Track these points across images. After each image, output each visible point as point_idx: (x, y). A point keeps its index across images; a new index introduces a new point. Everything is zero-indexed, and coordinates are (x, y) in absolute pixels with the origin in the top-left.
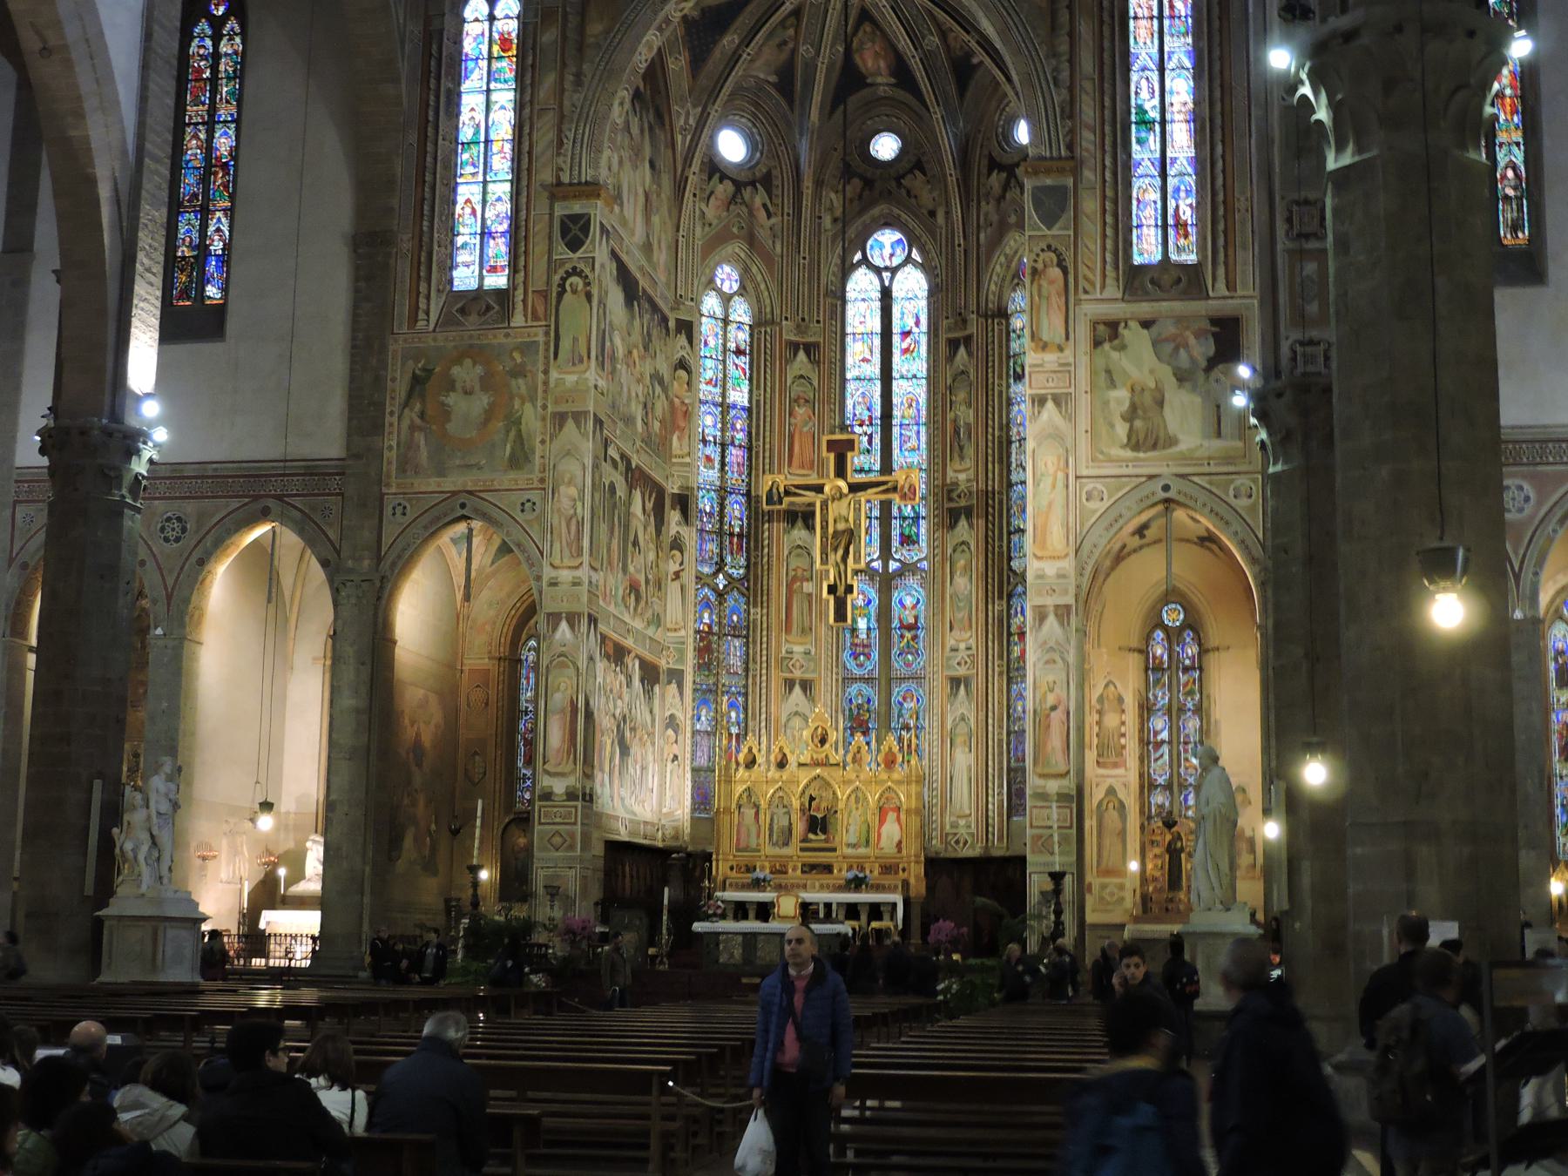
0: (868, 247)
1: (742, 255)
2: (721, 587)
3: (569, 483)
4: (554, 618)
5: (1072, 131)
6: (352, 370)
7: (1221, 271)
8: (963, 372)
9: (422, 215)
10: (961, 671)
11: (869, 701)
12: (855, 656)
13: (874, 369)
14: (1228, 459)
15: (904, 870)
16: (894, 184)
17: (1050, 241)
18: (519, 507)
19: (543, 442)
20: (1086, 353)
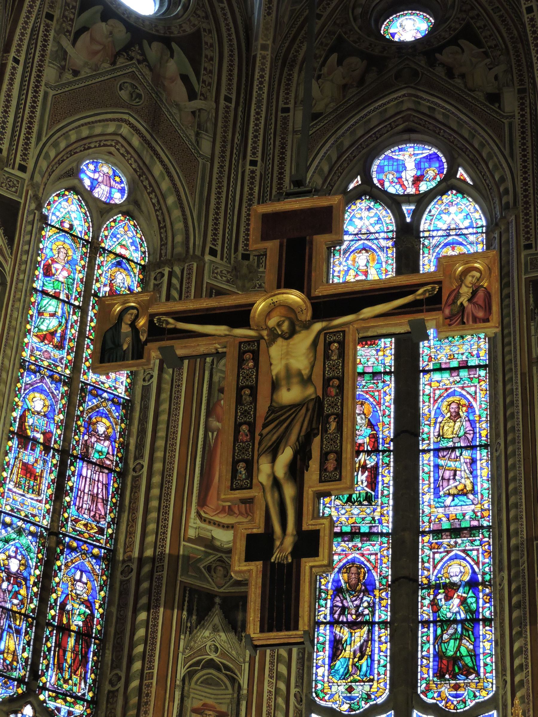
0: (374, 168)
1: (136, 141)
16: (423, 61)
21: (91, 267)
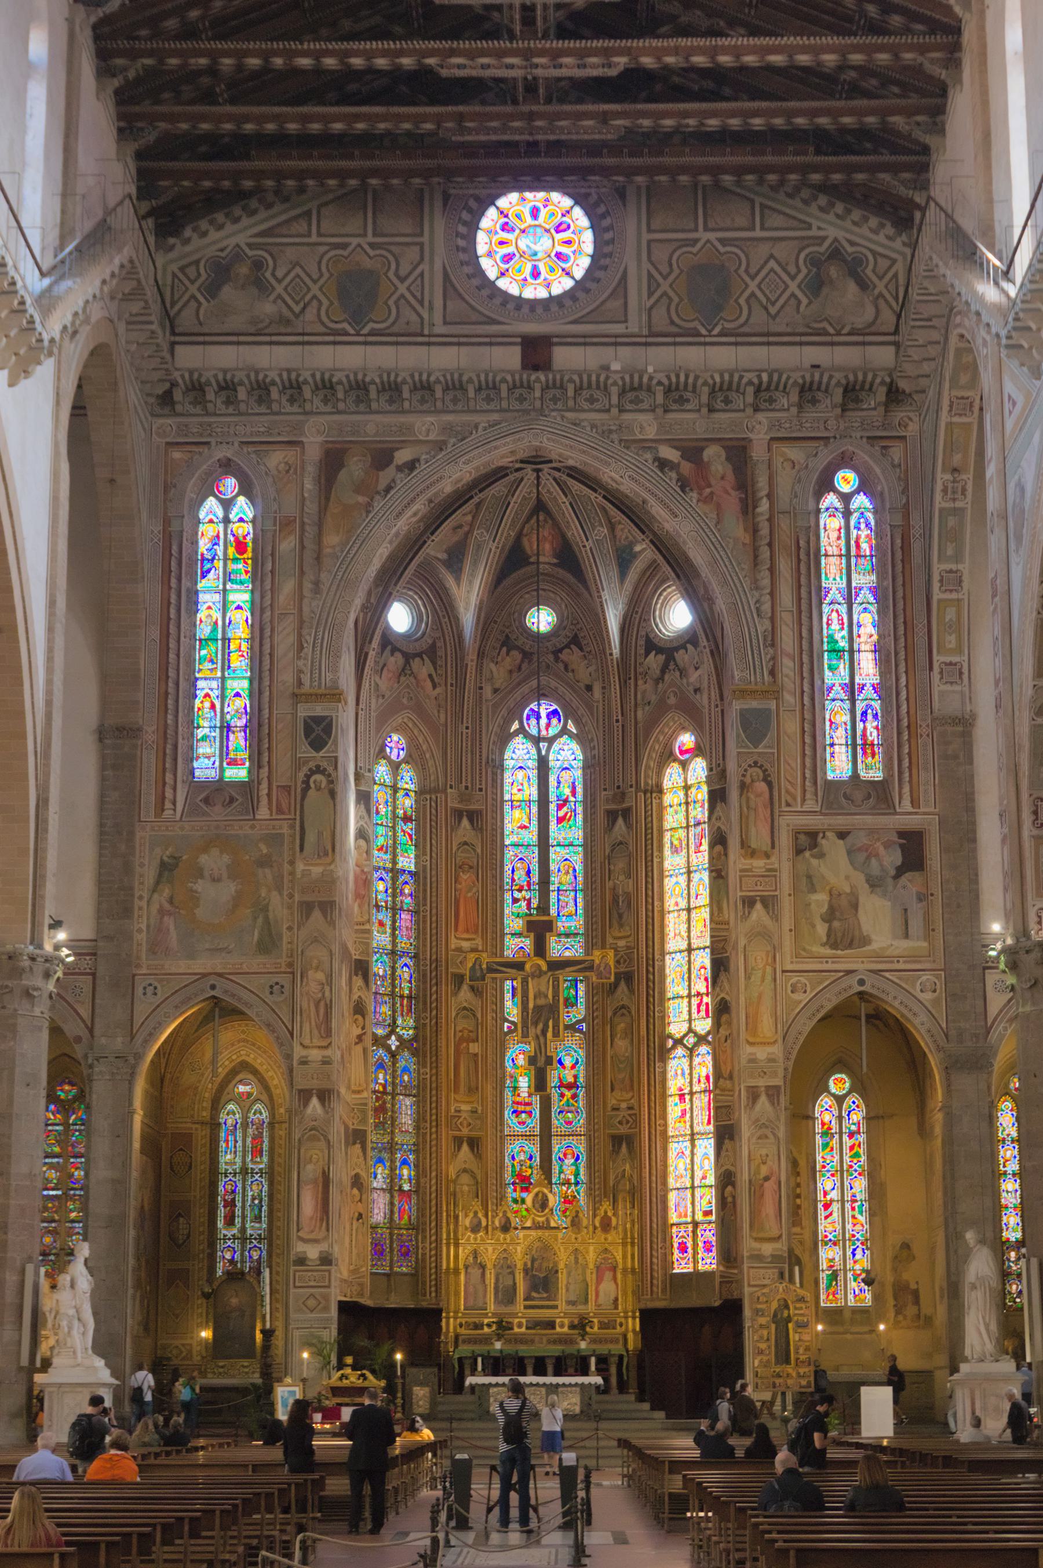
2: (393, 1048)
3: (317, 968)
4: (305, 1096)
5: (773, 658)
6: (101, 855)
7: (906, 789)
8: (621, 843)
9: (166, 709)
10: (623, 1130)
11: (531, 1158)
12: (516, 1112)
13: (531, 836)
14: (913, 958)
15: (621, 1325)
16: (551, 657)
17: (755, 758)
18: (267, 990)
19: (290, 928)
20: (789, 860)
21: (395, 799)
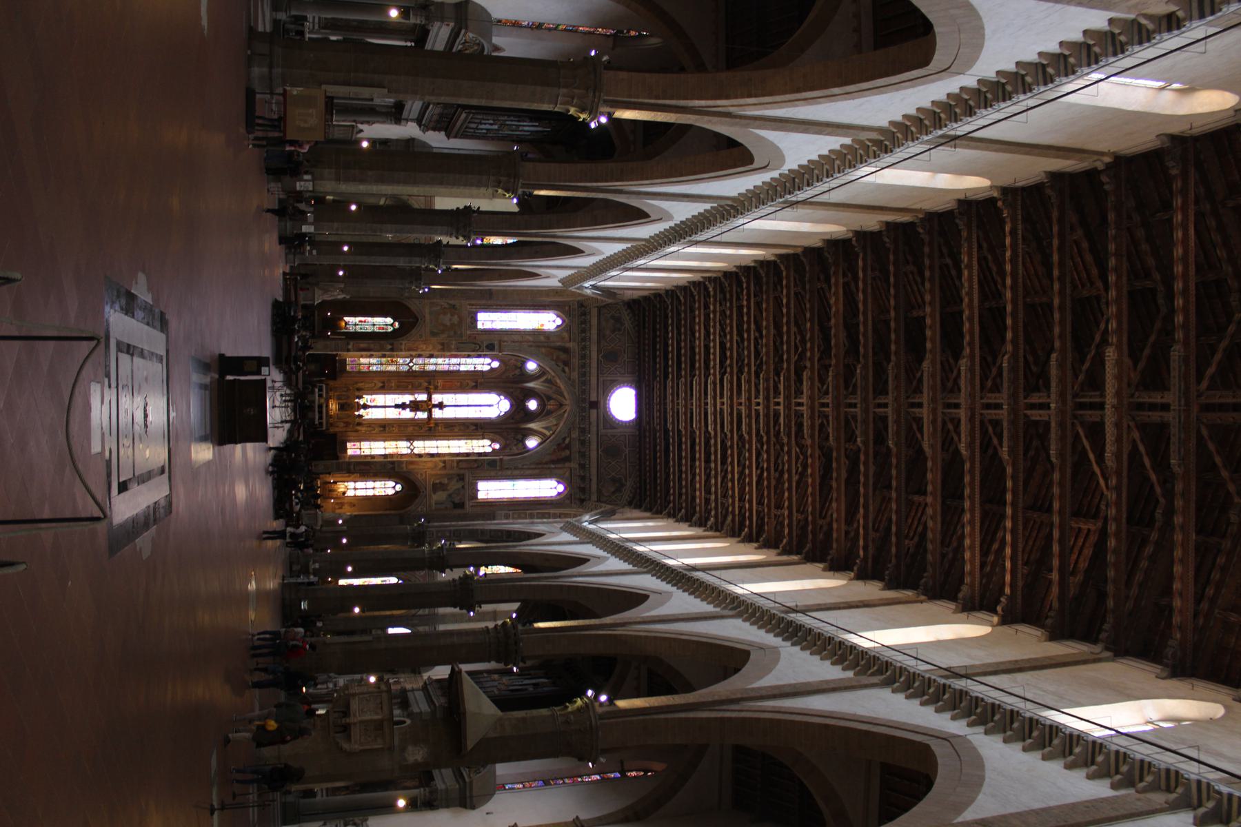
4: (392, 344)
10: (387, 429)
